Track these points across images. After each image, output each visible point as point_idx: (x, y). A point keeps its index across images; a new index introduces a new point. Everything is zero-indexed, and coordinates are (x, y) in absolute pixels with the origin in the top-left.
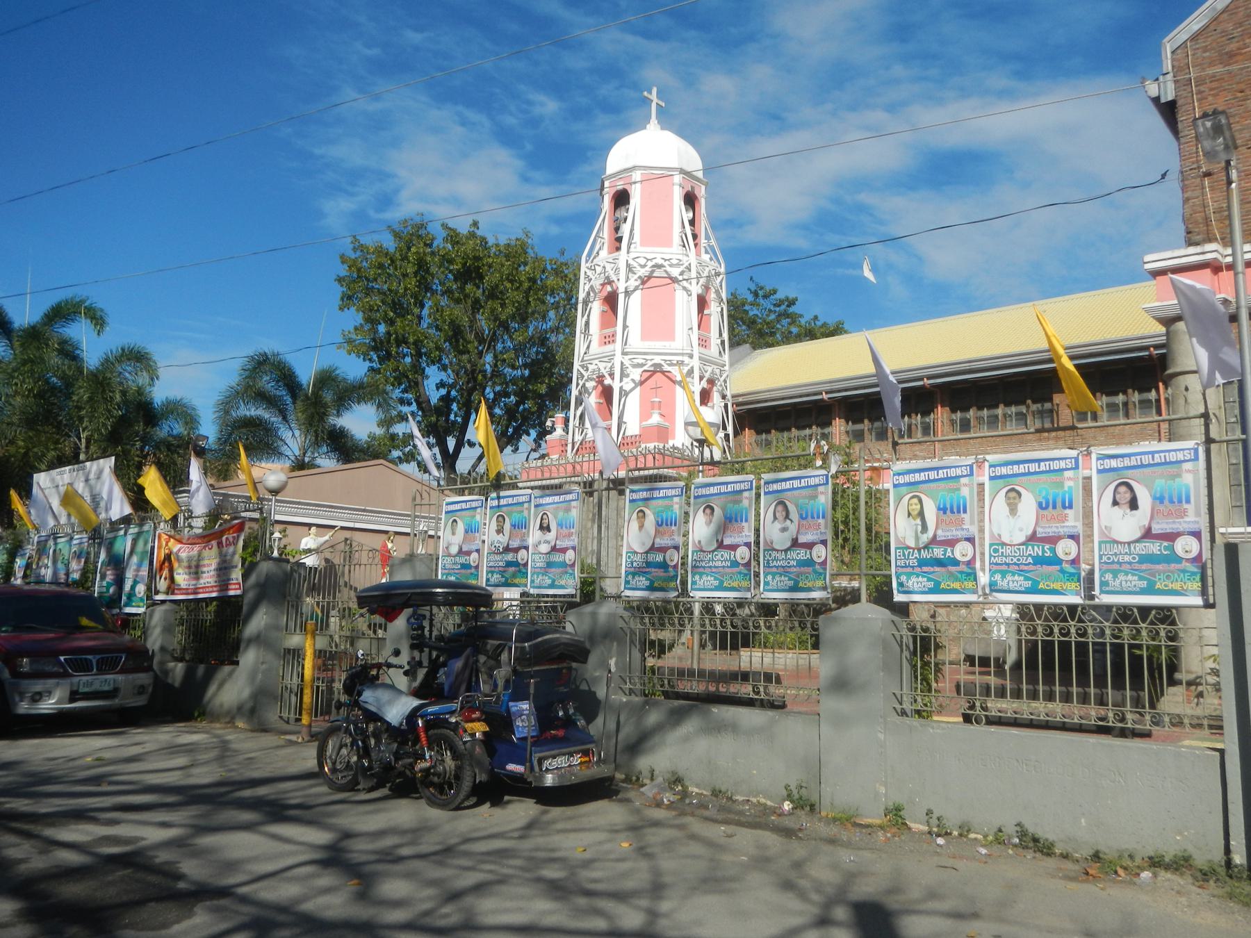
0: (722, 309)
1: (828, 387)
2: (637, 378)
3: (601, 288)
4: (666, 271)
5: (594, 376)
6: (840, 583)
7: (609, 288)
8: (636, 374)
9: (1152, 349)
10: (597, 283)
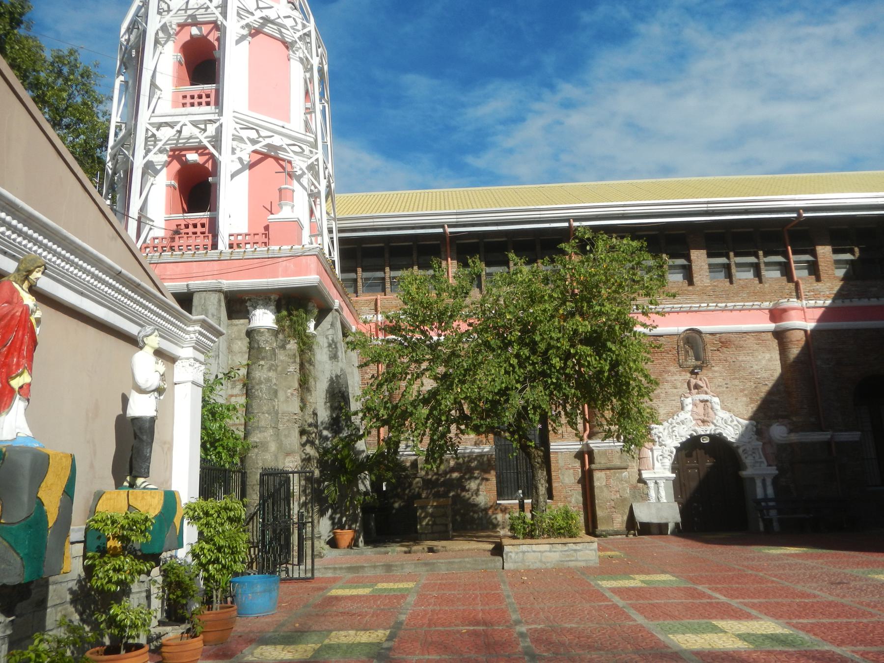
0: (324, 107)
1: (453, 219)
2: (246, 159)
3: (178, 29)
4: (281, 32)
5: (168, 147)
6: (466, 448)
7: (195, 31)
8: (246, 152)
9: (801, 211)
10: (173, 20)
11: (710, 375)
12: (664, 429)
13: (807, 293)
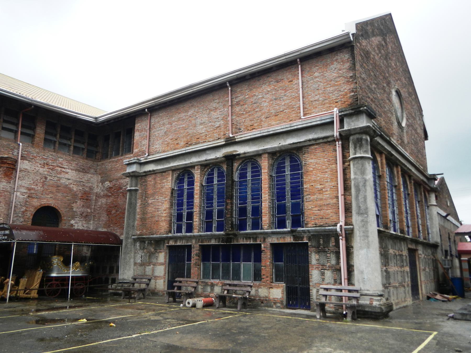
13: (23, 152)
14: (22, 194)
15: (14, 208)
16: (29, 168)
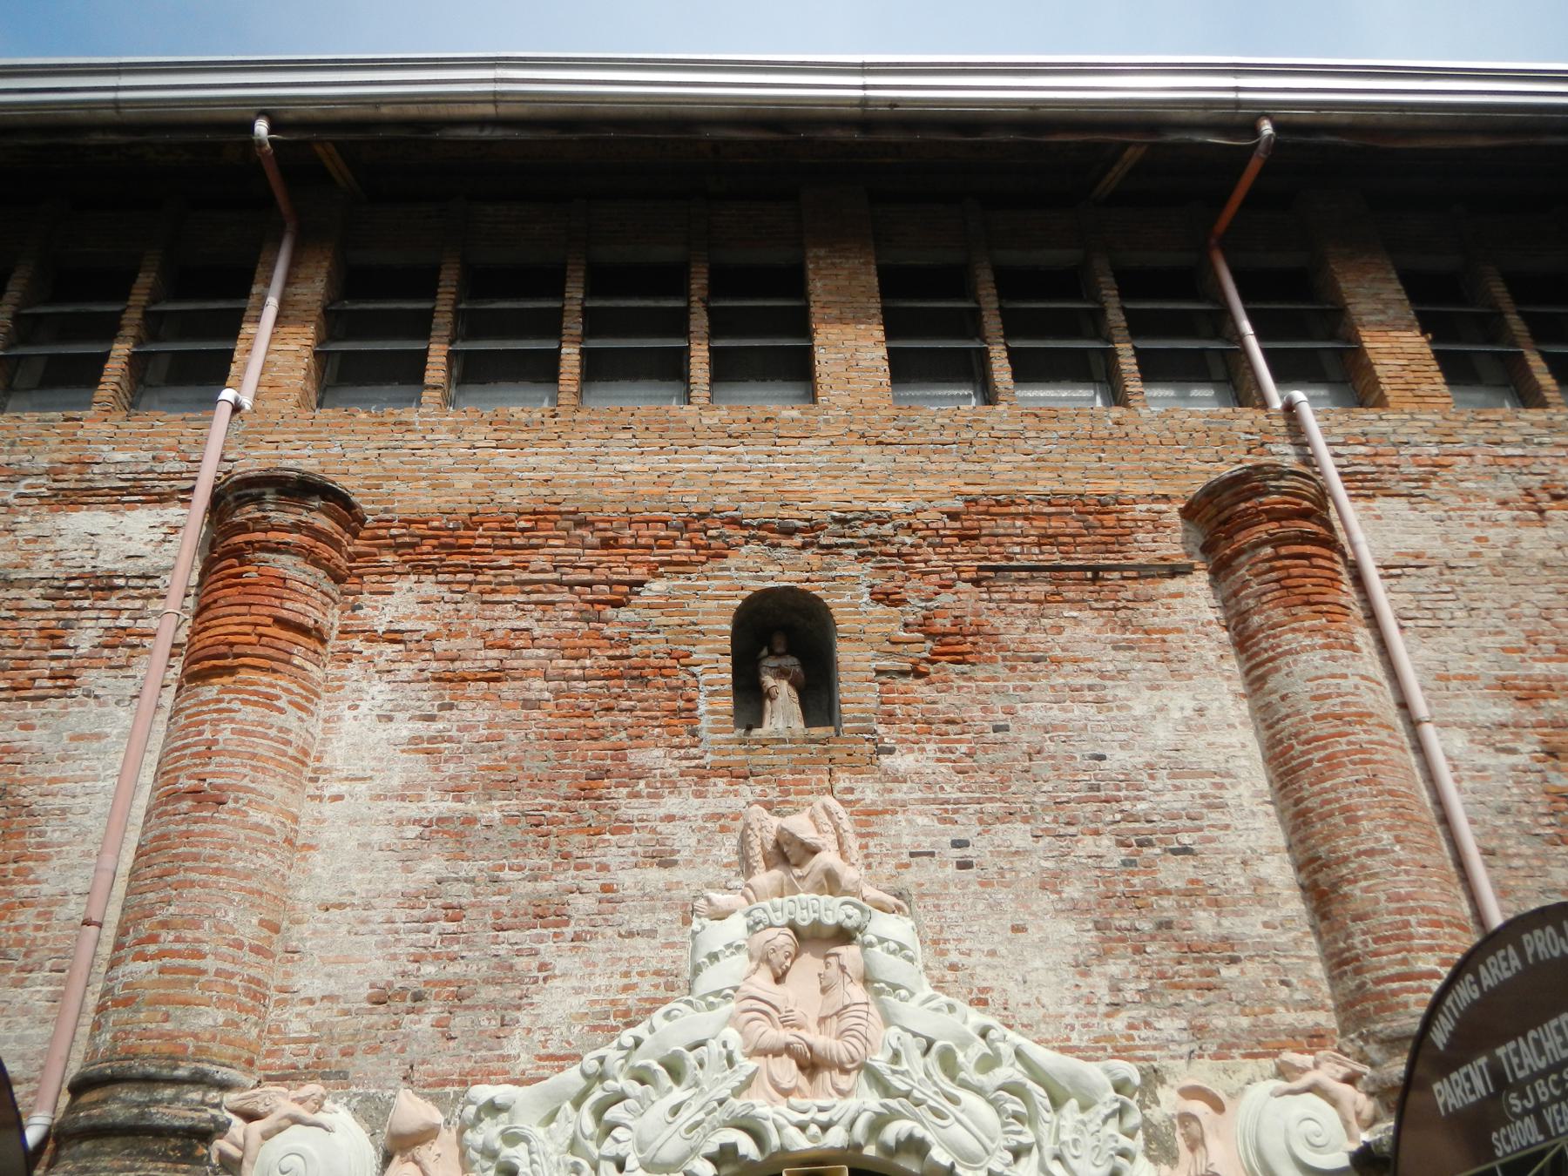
11: (869, 793)
12: (551, 1117)
13: (1338, 449)
14: (1492, 736)
15: (1489, 866)
16: (1436, 548)
